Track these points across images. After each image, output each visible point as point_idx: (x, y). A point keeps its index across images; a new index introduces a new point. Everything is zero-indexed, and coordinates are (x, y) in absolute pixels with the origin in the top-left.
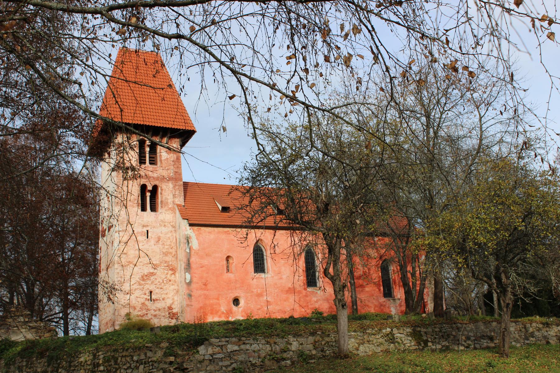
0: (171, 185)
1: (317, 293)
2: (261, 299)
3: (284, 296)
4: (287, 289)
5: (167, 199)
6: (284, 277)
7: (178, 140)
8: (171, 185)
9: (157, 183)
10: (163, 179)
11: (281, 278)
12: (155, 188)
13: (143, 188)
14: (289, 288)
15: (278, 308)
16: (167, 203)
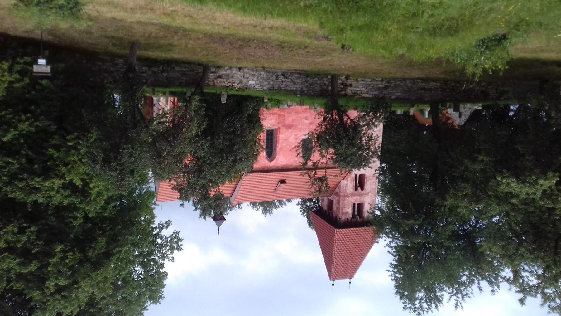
0: (348, 192)
1: (271, 125)
2: (311, 121)
3: (295, 123)
4: (292, 128)
5: (351, 183)
6: (293, 136)
7: (341, 222)
8: (348, 192)
9: (355, 192)
10: (353, 195)
11: (296, 135)
12: (356, 189)
13: (362, 189)
14: (290, 128)
15: (301, 115)
16: (351, 180)
